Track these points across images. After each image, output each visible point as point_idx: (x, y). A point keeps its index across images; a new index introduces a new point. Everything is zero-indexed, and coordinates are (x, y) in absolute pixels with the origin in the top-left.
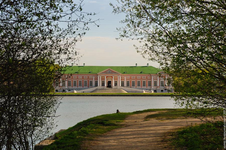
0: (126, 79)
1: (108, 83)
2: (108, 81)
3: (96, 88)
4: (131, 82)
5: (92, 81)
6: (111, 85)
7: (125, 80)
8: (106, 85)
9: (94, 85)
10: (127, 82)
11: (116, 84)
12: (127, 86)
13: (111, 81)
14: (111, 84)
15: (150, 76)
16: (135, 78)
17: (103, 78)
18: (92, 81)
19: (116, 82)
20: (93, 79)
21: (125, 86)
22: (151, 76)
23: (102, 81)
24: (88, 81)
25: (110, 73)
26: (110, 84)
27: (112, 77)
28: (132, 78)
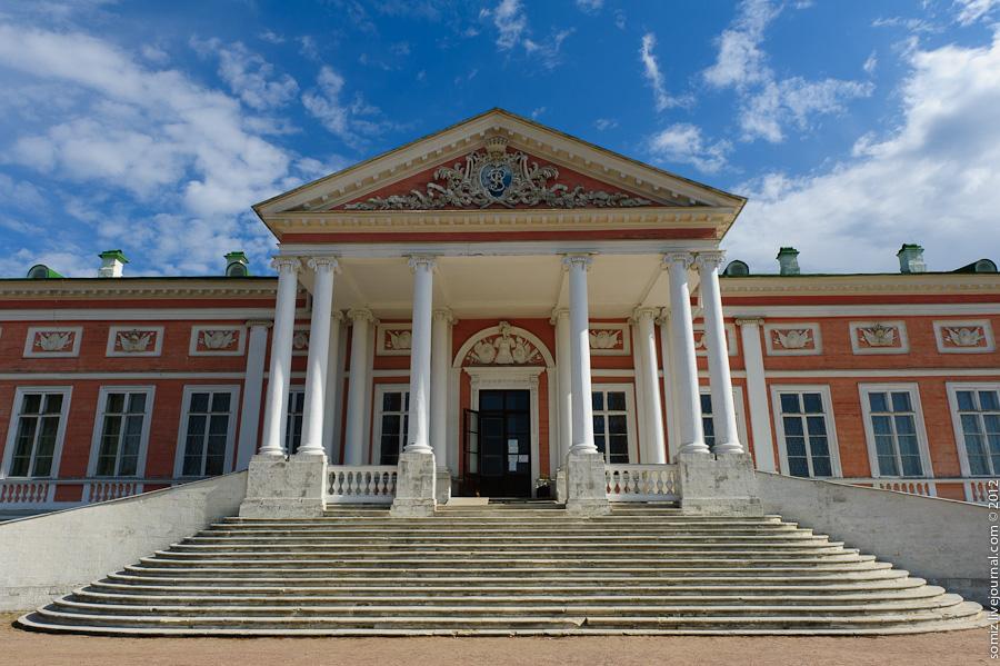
0: (769, 363)
1: (480, 414)
2: (476, 388)
4: (847, 406)
5: (222, 401)
6: (525, 468)
8: (429, 440)
10: (789, 402)
13: (528, 391)
14: (525, 449)
16: (904, 348)
18: (234, 390)
20: (240, 364)
23: (382, 390)
24: (168, 393)
25: (520, 206)
26: (513, 446)
27: (545, 328)
28: (856, 350)
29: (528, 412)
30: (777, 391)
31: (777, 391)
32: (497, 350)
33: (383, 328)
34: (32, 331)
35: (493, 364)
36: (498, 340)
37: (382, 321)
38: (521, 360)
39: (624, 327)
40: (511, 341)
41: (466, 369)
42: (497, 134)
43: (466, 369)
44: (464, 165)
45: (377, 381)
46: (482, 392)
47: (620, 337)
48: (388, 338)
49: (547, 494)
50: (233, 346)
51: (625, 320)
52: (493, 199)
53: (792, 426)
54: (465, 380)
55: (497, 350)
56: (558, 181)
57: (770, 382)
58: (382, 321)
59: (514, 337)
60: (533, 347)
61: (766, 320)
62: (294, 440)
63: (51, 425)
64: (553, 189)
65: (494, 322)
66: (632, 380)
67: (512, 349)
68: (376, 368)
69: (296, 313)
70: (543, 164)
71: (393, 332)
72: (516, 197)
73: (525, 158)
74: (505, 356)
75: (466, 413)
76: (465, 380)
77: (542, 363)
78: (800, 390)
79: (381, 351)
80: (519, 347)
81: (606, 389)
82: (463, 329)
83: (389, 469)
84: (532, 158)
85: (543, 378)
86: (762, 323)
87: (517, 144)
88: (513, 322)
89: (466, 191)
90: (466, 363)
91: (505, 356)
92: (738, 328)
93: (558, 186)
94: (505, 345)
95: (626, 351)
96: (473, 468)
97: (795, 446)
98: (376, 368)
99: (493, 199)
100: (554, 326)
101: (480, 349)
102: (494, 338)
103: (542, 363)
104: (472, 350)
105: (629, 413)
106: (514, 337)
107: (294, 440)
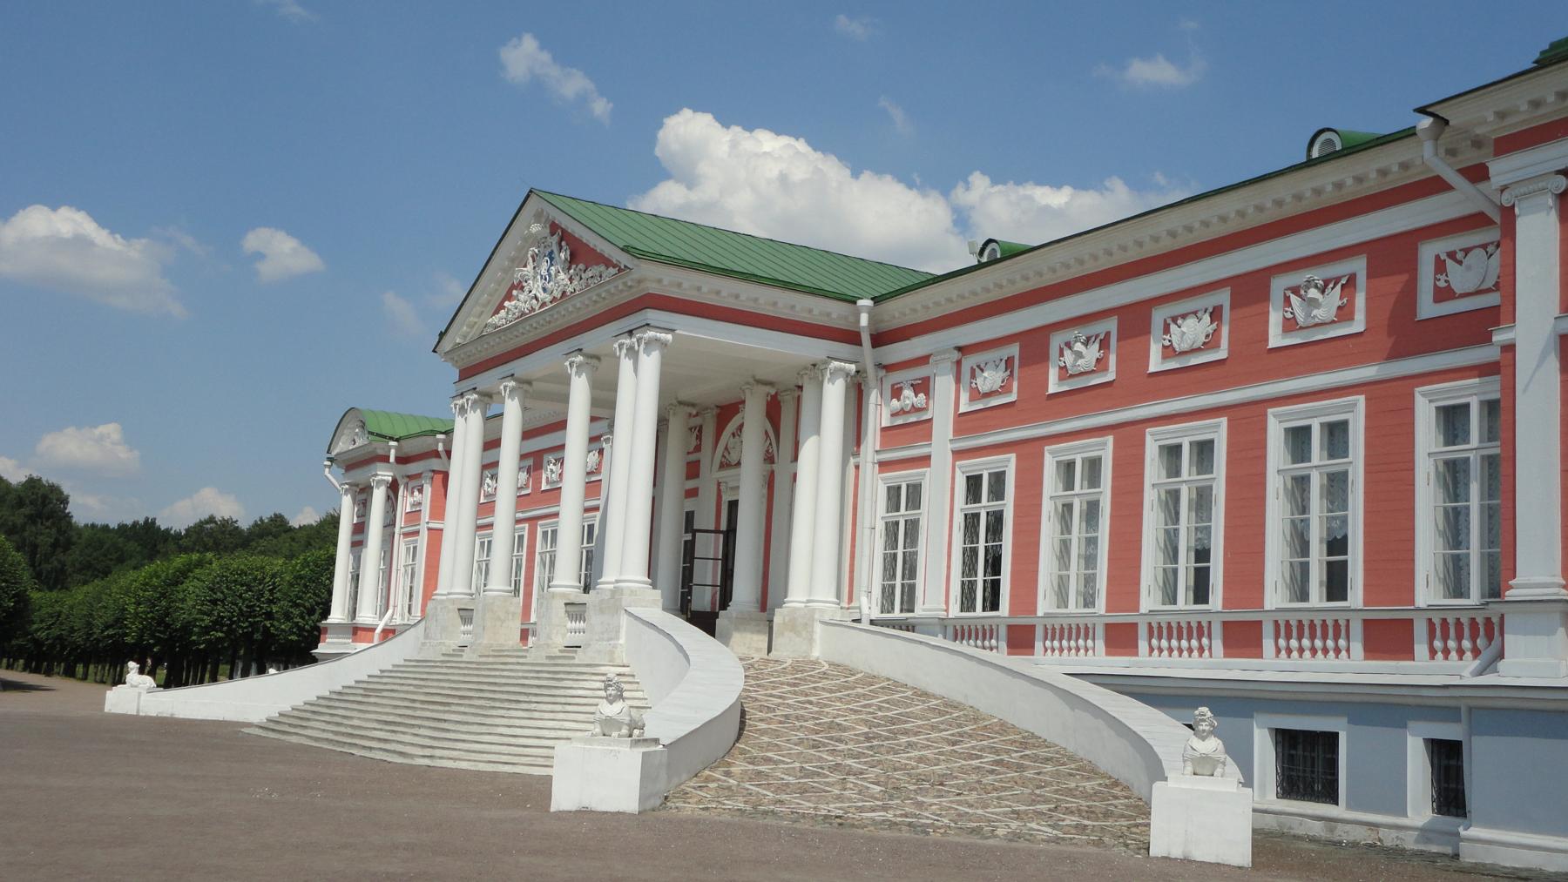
0: (964, 424)
7: (942, 440)
34: (1429, 252)
57: (959, 454)
69: (590, 430)
78: (984, 466)
86: (956, 355)
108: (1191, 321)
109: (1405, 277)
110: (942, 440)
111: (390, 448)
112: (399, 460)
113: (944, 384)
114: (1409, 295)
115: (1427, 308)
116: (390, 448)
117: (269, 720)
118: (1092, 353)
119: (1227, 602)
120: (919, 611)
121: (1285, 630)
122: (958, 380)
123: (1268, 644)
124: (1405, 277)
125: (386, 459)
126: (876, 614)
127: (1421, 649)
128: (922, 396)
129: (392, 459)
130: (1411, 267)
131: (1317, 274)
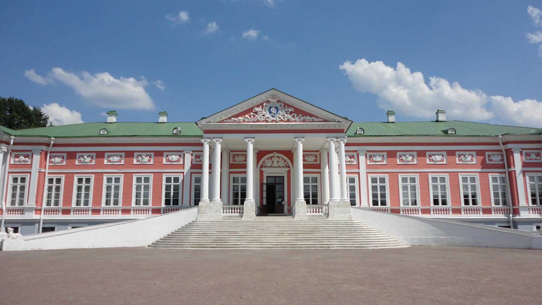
0: (368, 166)
2: (265, 175)
3: (195, 210)
7: (363, 170)
9: (186, 202)
10: (374, 180)
11: (313, 198)
12: (375, 203)
13: (283, 177)
15: (502, 147)
17: (239, 160)
19: (310, 184)
21: (364, 204)
22: (509, 146)
23: (232, 176)
27: (290, 154)
29: (283, 184)
30: (370, 176)
31: (370, 176)
32: (273, 162)
33: (232, 153)
35: (271, 167)
36: (273, 158)
37: (232, 151)
38: (281, 165)
39: (318, 153)
40: (278, 158)
41: (263, 169)
42: (273, 97)
43: (263, 169)
44: (263, 106)
45: (230, 173)
46: (267, 177)
47: (316, 157)
48: (234, 157)
49: (291, 213)
50: (178, 161)
51: (318, 151)
52: (272, 118)
53: (374, 188)
54: (261, 172)
55: (273, 162)
56: (294, 112)
58: (232, 151)
59: (279, 157)
60: (285, 161)
61: (368, 151)
62: (211, 197)
63: (117, 188)
64: (292, 115)
65: (272, 152)
66: (320, 173)
67: (278, 162)
68: (230, 168)
70: (289, 106)
71: (236, 155)
72: (279, 118)
73: (283, 104)
74: (275, 164)
75: (262, 184)
76: (261, 172)
77: (289, 167)
78: (378, 176)
79: (232, 162)
80: (280, 161)
81: (311, 176)
82: (260, 155)
83: (241, 206)
84: (285, 104)
85: (289, 172)
86: (366, 152)
87: (280, 99)
88: (278, 152)
89: (263, 116)
90: (261, 167)
91: (275, 164)
92: (358, 155)
93: (294, 114)
94: (275, 160)
95: (318, 162)
96: (265, 203)
97: (375, 196)
98: (230, 168)
99: (272, 118)
100: (292, 154)
101: (266, 161)
102: (272, 157)
103: (289, 167)
104: (264, 162)
105: (318, 184)
106: (279, 157)
107: (211, 197)
108: (437, 156)
109: (482, 157)
110: (363, 170)
111: (11, 139)
112: (15, 144)
113: (362, 159)
114: (485, 159)
115: (488, 162)
116: (11, 139)
117: (161, 239)
118: (410, 158)
119: (123, 204)
120: (358, 205)
121: (466, 210)
122: (366, 157)
123: (463, 212)
124: (482, 157)
125: (8, 143)
126: (9, 205)
127: (493, 213)
128: (353, 159)
129: (12, 143)
130: (484, 156)
131: (467, 153)
